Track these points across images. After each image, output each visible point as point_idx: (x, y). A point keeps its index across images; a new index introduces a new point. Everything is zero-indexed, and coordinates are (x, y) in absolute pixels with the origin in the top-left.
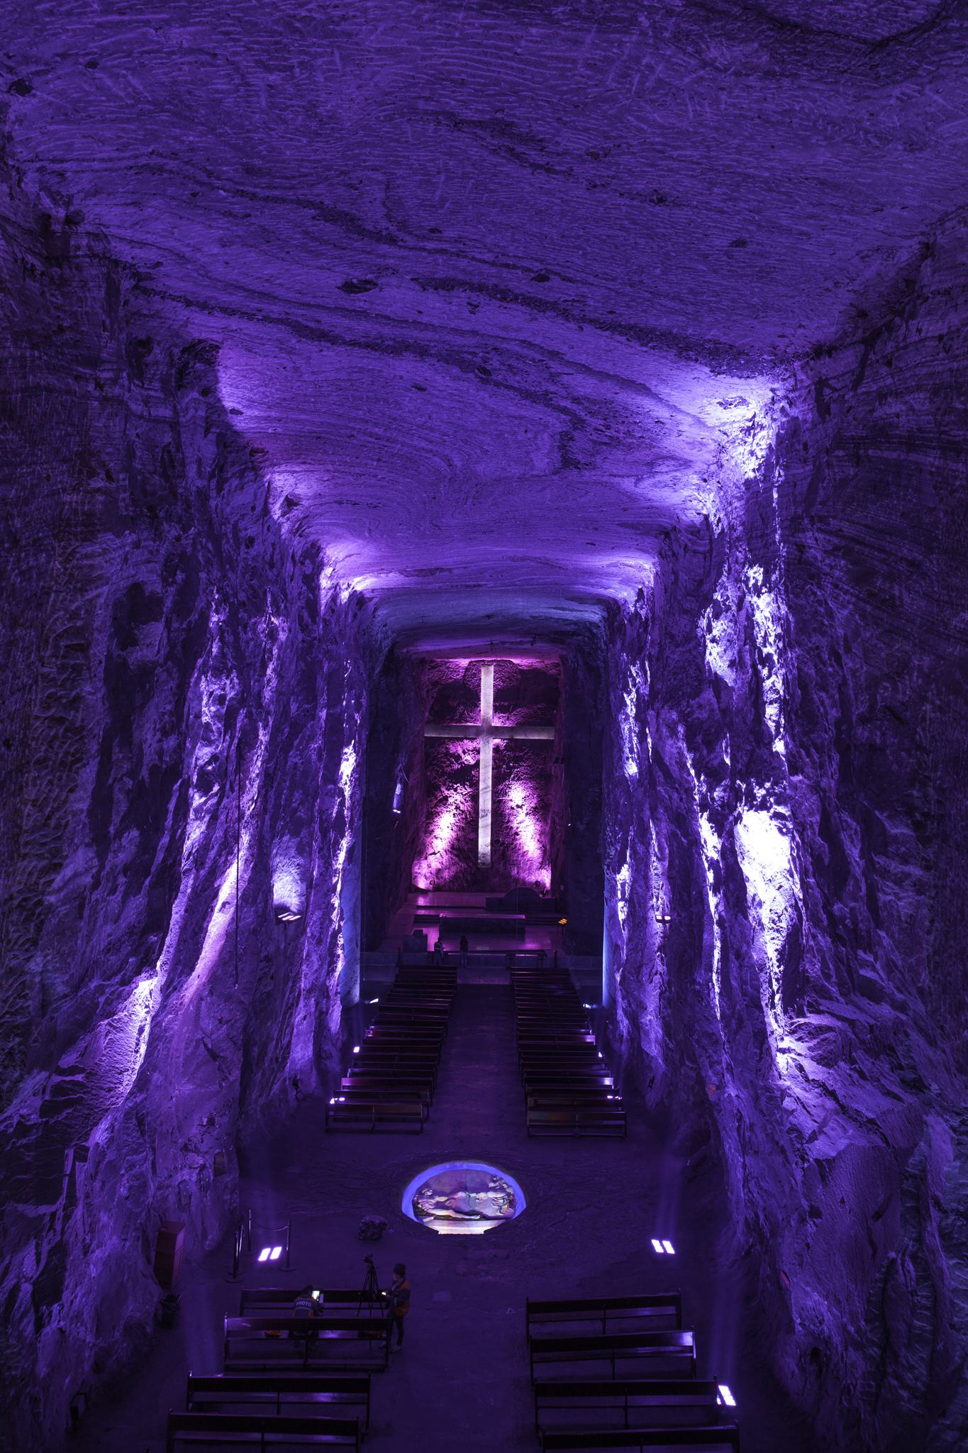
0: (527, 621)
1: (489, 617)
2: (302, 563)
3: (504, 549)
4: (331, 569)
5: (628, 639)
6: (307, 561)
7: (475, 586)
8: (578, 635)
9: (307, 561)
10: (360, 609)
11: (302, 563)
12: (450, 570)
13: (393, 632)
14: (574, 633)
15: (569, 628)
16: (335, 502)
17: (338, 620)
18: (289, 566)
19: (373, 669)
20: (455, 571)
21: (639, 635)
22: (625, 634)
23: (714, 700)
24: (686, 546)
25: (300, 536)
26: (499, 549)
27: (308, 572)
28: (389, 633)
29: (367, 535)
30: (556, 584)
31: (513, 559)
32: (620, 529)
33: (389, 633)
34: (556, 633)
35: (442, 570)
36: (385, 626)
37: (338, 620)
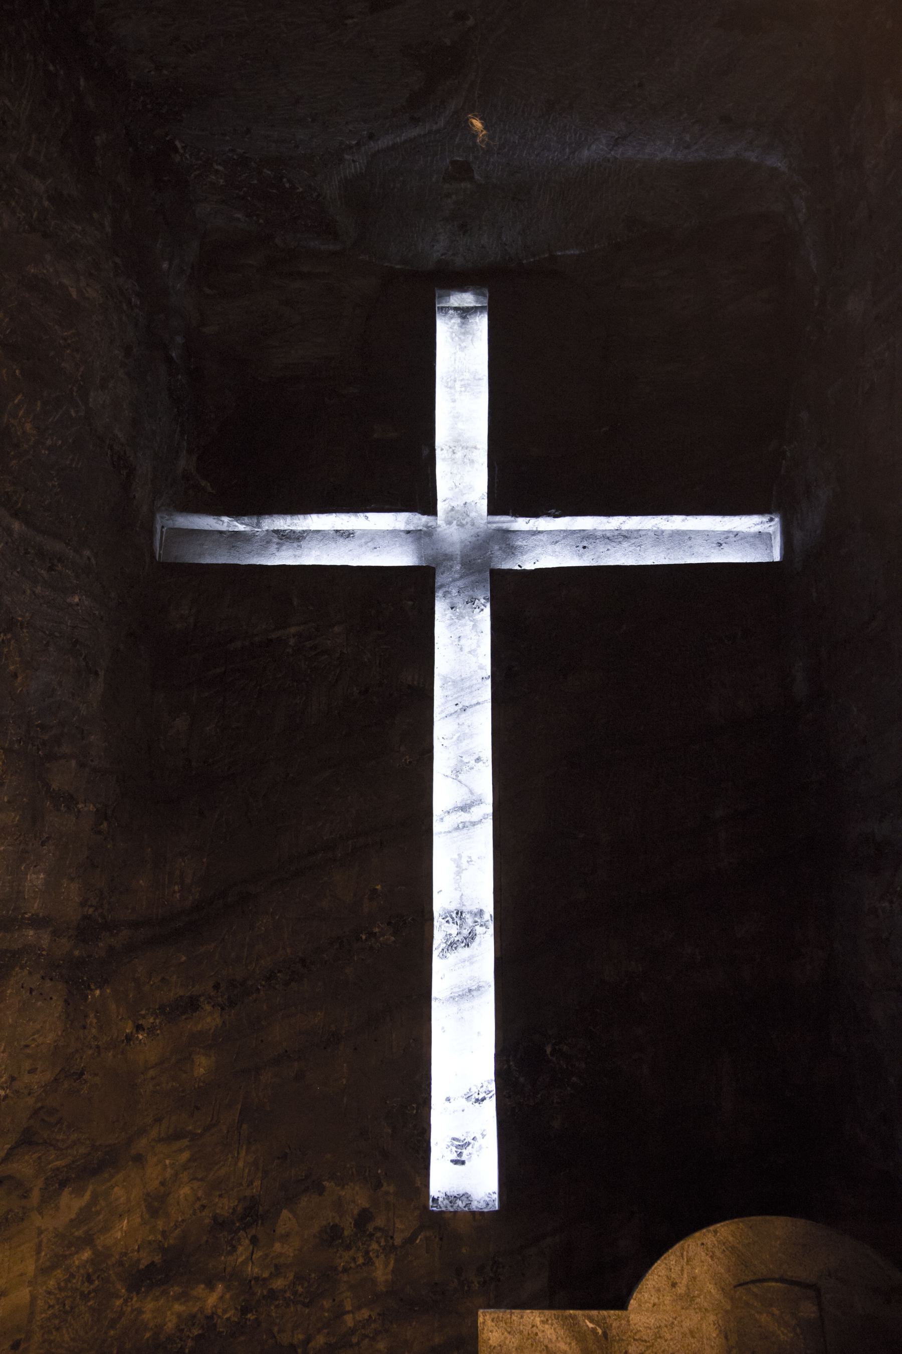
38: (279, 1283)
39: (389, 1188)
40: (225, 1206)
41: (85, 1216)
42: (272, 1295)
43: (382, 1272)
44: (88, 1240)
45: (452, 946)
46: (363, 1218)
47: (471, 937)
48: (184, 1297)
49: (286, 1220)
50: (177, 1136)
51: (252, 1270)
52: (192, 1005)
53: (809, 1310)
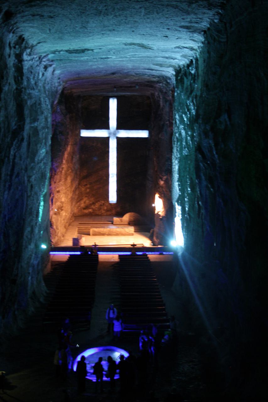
0: (134, 76)
1: (113, 74)
2: (15, 47)
3: (121, 39)
4: (30, 50)
5: (185, 86)
6: (17, 47)
7: (106, 58)
8: (160, 83)
9: (17, 47)
10: (45, 71)
11: (15, 47)
12: (92, 50)
13: (63, 82)
14: (158, 82)
15: (155, 80)
16: (31, 15)
17: (34, 77)
18: (7, 50)
19: (53, 102)
20: (95, 51)
21: (191, 84)
22: (183, 83)
23: (227, 119)
24: (215, 38)
25: (13, 33)
26: (118, 39)
27: (17, 52)
28: (61, 82)
29: (48, 32)
30: (148, 57)
31: (126, 44)
32: (180, 29)
33: (61, 82)
34: (148, 82)
35: (88, 50)
36: (59, 79)
37: (34, 77)
38: (96, 209)
39: (106, 201)
40: (91, 203)
41: (79, 204)
42: (96, 210)
43: (105, 208)
44: (80, 206)
45: (112, 177)
46: (104, 204)
47: (113, 176)
48: (88, 210)
49: (97, 204)
50: (86, 197)
51: (94, 208)
52: (86, 185)
53: (134, 218)
